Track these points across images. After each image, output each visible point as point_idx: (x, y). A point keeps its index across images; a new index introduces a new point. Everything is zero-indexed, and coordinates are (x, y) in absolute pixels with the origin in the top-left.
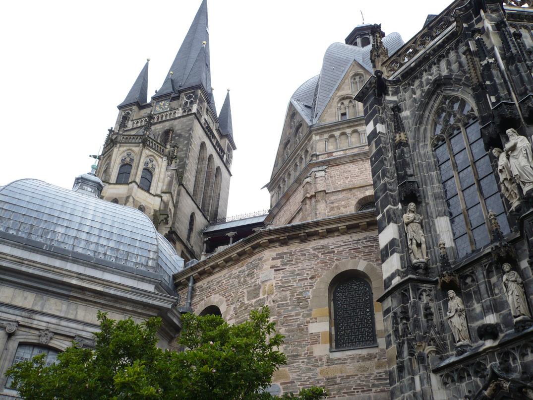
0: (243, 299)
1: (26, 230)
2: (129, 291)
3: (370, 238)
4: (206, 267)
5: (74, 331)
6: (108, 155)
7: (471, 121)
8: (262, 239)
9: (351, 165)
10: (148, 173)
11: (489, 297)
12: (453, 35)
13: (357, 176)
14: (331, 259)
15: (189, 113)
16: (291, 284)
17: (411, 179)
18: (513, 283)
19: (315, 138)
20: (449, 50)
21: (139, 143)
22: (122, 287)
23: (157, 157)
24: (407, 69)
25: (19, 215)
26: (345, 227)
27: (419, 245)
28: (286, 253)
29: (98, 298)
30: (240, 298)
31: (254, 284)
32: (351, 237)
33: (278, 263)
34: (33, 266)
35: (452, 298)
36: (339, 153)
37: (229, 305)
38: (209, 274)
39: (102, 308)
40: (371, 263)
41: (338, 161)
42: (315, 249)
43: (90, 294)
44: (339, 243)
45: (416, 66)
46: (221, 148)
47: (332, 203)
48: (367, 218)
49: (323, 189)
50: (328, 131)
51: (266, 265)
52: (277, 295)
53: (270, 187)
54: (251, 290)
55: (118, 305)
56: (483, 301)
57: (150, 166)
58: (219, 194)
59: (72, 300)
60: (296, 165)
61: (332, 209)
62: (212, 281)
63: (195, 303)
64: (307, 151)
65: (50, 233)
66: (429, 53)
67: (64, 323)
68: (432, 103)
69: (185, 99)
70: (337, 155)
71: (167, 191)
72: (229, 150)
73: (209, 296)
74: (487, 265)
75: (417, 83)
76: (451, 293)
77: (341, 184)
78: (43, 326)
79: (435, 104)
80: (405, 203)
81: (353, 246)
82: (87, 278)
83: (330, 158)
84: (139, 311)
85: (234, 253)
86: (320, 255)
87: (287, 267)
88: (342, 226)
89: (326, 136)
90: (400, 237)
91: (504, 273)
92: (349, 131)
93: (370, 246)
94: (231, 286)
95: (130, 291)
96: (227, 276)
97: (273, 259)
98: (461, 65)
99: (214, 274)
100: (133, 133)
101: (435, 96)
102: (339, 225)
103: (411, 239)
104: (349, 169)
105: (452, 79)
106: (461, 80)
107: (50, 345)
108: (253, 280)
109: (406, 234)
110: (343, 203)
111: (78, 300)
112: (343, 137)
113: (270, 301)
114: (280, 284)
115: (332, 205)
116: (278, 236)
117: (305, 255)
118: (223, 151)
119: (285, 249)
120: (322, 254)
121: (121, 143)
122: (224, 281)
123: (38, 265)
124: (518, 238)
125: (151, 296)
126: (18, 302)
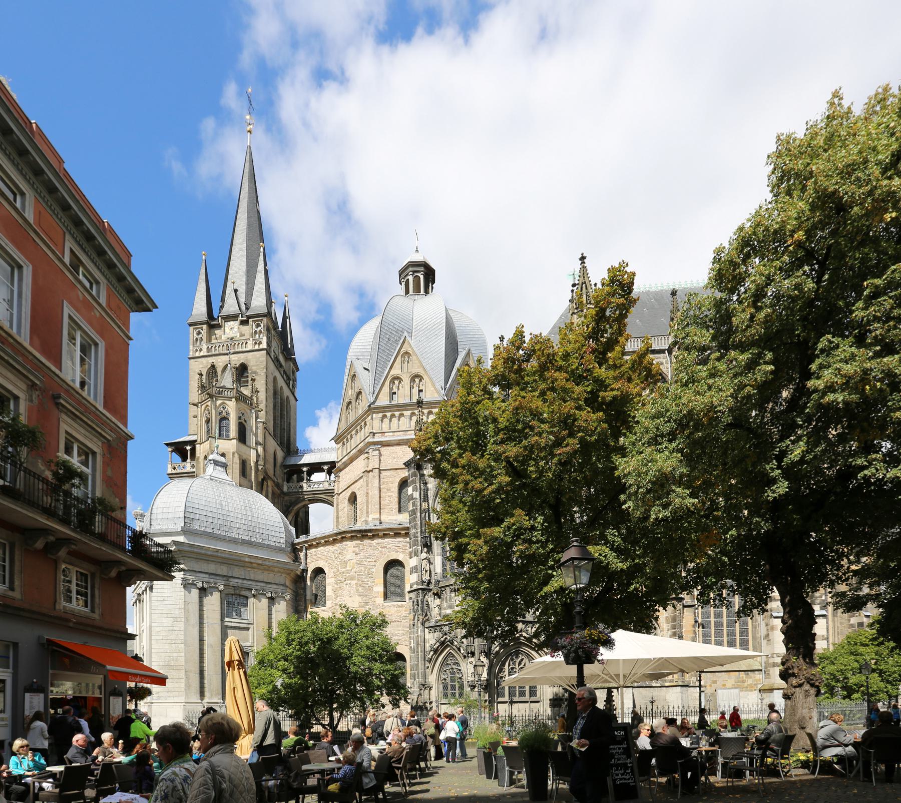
27: (426, 571)
33: (357, 549)
49: (378, 466)
72: (294, 373)
87: (362, 553)
118: (289, 378)
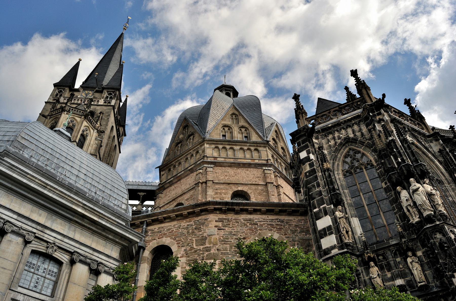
0: (193, 245)
1: (44, 161)
2: (115, 224)
3: (280, 219)
4: (160, 217)
5: (73, 248)
6: (55, 117)
7: (369, 166)
8: (210, 206)
9: (229, 168)
10: (84, 137)
11: (397, 269)
12: (358, 117)
13: (233, 176)
14: (255, 228)
15: (109, 104)
16: (230, 240)
17: (338, 192)
18: (416, 263)
19: (206, 146)
20: (354, 123)
21: (81, 116)
22: (111, 221)
23: (91, 129)
24: (326, 127)
25: (39, 148)
26: (265, 210)
27: (347, 232)
28: (225, 219)
29: (92, 225)
30: (190, 243)
31: (201, 236)
32: (268, 217)
33: (220, 224)
34: (53, 191)
35: (372, 267)
36: (221, 159)
37: (180, 247)
38: (160, 222)
39: (92, 233)
40: (282, 236)
41: (221, 164)
42: (244, 220)
43: (87, 221)
44: (260, 219)
45: (332, 126)
46: (119, 133)
47: (217, 190)
48: (280, 207)
49: (212, 179)
50: (215, 143)
51: (211, 224)
52: (220, 246)
53: (161, 168)
54: (198, 240)
55: (104, 234)
56: (393, 271)
57: (85, 133)
58: (113, 163)
59: (73, 224)
60: (187, 159)
61: (216, 193)
62: (162, 227)
63: (148, 241)
64: (197, 152)
65: (60, 168)
66: (342, 122)
67: (66, 240)
68: (342, 150)
69: (106, 94)
70: (220, 160)
71: (94, 154)
73: (161, 238)
74: (393, 250)
75: (330, 136)
76: (372, 264)
77: (222, 179)
78: (51, 240)
79: (345, 151)
80: (336, 206)
81: (269, 223)
82: (89, 209)
83: (215, 161)
84: (117, 240)
85: (185, 212)
86: (248, 224)
87: (227, 228)
88: (263, 209)
89: (213, 146)
90: (333, 225)
91: (407, 256)
92: (228, 147)
93: (280, 225)
94: (181, 234)
95: (116, 225)
96: (176, 226)
97: (216, 221)
98: (362, 135)
99: (164, 223)
100: (74, 106)
101: (344, 147)
102: (262, 208)
103: (343, 228)
104: (228, 171)
105: (358, 140)
106: (364, 143)
107: (54, 255)
108: (200, 233)
109: (339, 224)
110: (224, 191)
111: (77, 224)
112: (224, 150)
113: (215, 249)
114: (222, 239)
115: (216, 191)
116: (221, 207)
117: (238, 223)
118: (120, 135)
119: (224, 216)
120: (250, 224)
121: (67, 112)
122: (174, 229)
123: (57, 192)
124: (415, 238)
125: (128, 231)
126: (35, 217)
